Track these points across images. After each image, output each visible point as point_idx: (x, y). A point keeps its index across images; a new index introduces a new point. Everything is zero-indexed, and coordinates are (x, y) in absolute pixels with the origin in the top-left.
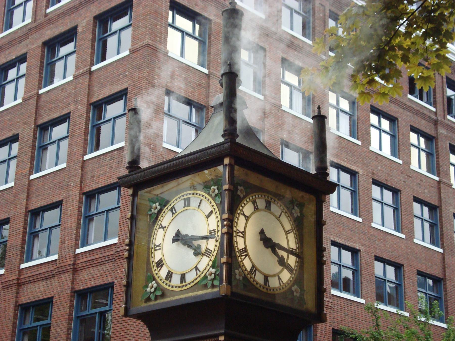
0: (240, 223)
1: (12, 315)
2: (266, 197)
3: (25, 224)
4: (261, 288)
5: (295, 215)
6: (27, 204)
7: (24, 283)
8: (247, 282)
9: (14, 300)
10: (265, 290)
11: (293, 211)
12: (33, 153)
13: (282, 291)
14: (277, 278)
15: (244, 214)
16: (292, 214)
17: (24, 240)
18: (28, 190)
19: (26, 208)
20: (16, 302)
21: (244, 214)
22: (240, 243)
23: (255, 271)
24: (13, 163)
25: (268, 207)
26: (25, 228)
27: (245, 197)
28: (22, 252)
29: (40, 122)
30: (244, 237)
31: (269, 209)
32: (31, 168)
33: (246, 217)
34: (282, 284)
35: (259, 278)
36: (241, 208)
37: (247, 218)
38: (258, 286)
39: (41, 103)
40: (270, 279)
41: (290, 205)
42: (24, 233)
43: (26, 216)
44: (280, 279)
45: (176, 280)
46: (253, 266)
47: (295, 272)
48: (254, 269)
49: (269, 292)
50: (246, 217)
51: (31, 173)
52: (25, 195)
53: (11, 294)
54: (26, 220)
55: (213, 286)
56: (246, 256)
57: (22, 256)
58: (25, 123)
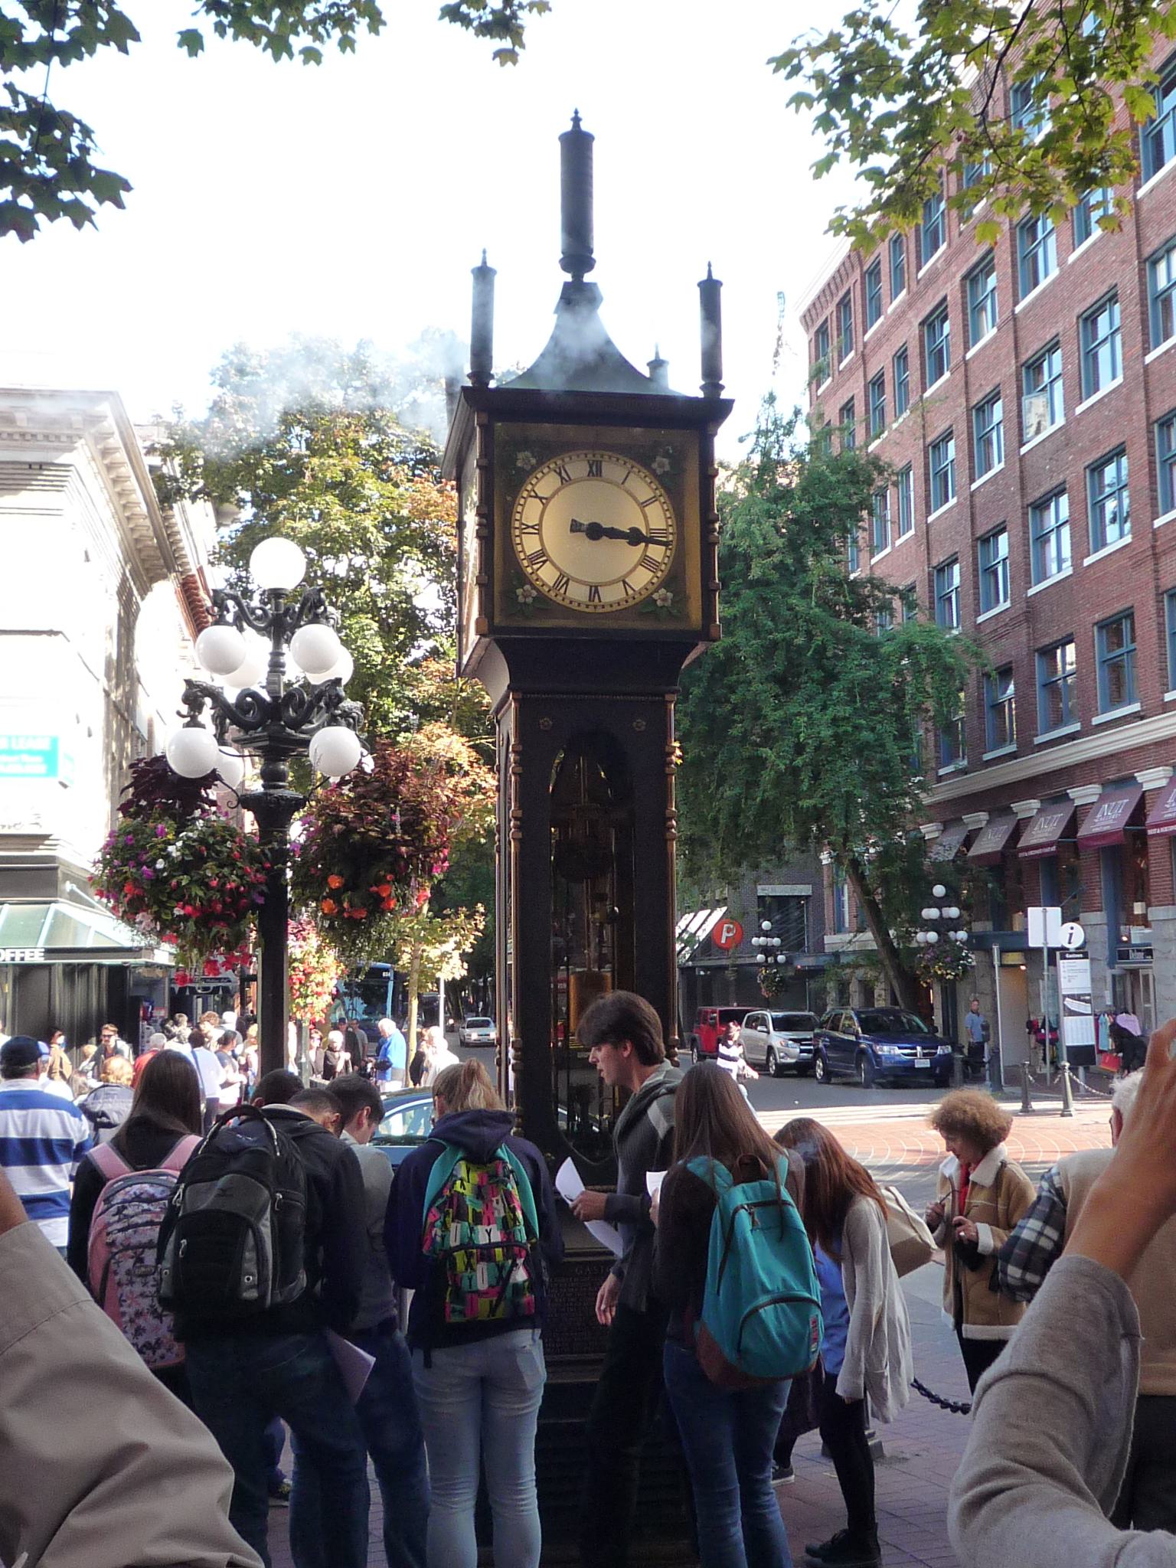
0: (529, 511)
1: (1153, 610)
2: (590, 456)
3: (1151, 446)
4: (583, 608)
5: (659, 471)
6: (1148, 410)
7: (1165, 552)
8: (544, 603)
9: (1152, 585)
10: (591, 610)
11: (655, 466)
12: (1144, 313)
13: (631, 602)
15: (536, 496)
16: (653, 472)
17: (1152, 475)
18: (1146, 383)
19: (1148, 417)
20: (1157, 587)
21: (536, 496)
22: (530, 545)
23: (567, 583)
24: (1118, 338)
25: (595, 472)
26: (1152, 455)
28: (1154, 499)
29: (1147, 251)
30: (539, 533)
31: (599, 473)
32: (1145, 341)
33: (541, 499)
34: (630, 592)
35: (577, 593)
36: (529, 487)
37: (545, 501)
38: (574, 606)
39: (1144, 215)
41: (643, 458)
42: (1151, 463)
43: (1150, 432)
44: (624, 582)
46: (562, 575)
48: (564, 580)
49: (600, 610)
50: (541, 499)
51: (1146, 351)
52: (1143, 393)
53: (1146, 572)
54: (1151, 440)
57: (1154, 505)
58: (1123, 262)
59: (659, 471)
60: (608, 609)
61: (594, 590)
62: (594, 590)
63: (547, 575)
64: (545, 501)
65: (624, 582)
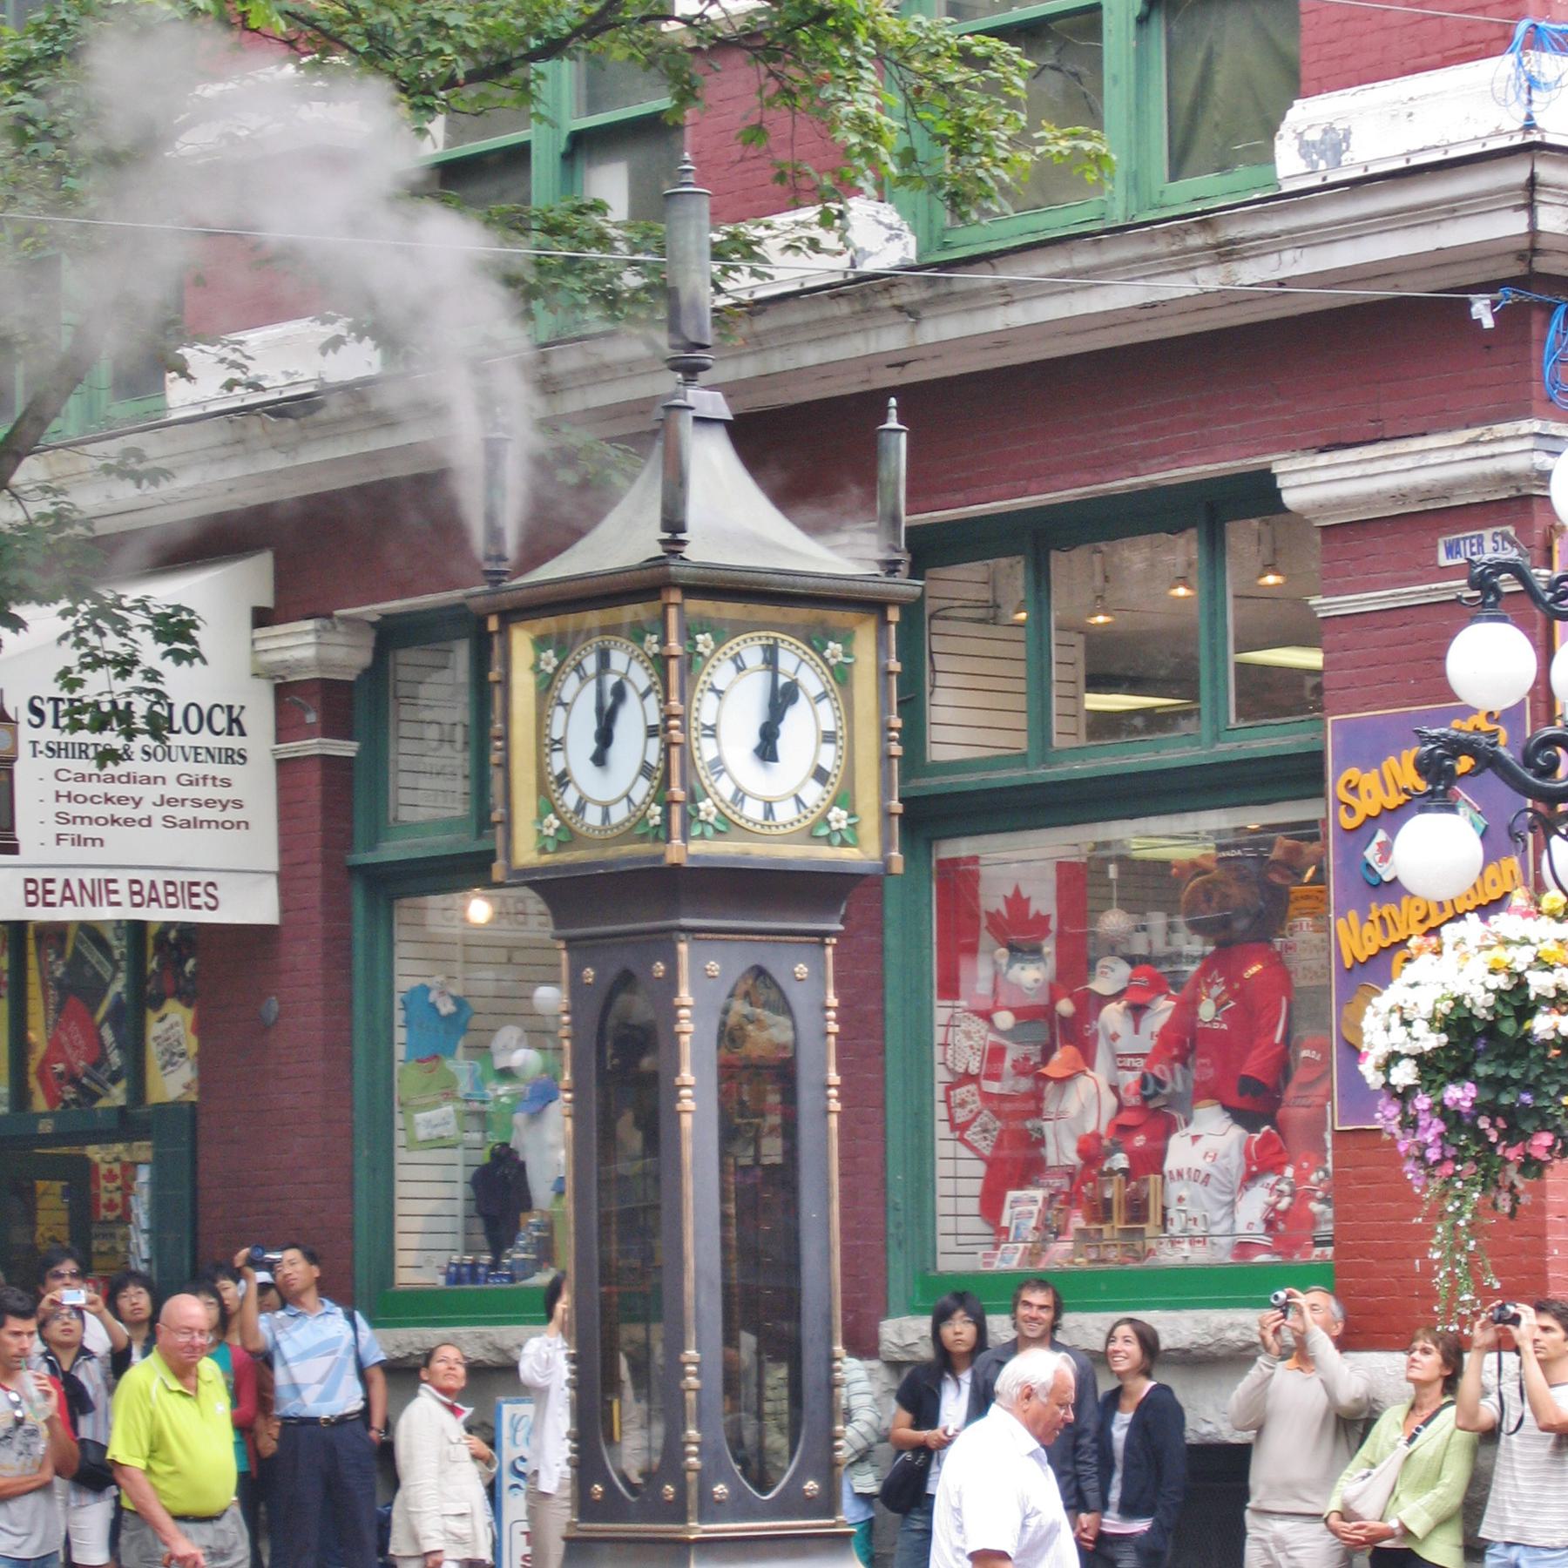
5: (833, 661)
11: (827, 653)
14: (792, 802)
15: (713, 689)
21: (713, 689)
27: (714, 652)
35: (753, 810)
40: (775, 806)
44: (798, 800)
45: (593, 816)
46: (738, 790)
47: (832, 779)
48: (740, 796)
50: (719, 693)
55: (657, 839)
56: (721, 772)
59: (833, 661)
60: (782, 830)
61: (769, 811)
62: (769, 811)
63: (725, 788)
64: (719, 693)
65: (798, 800)
